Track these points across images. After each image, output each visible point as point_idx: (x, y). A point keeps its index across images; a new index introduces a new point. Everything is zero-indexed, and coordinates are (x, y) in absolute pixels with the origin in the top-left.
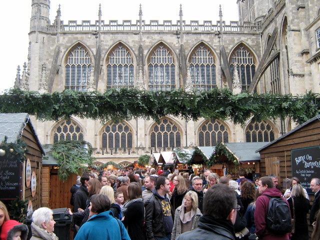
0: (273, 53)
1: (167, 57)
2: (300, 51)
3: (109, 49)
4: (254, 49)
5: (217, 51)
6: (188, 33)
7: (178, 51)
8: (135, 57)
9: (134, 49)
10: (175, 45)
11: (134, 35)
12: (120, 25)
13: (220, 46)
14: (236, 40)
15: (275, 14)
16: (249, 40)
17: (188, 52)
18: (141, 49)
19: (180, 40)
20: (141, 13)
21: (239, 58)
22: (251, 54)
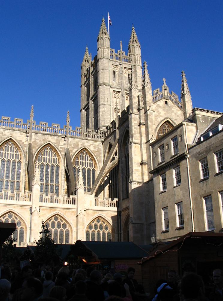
1: (15, 153)
2: (140, 161)
4: (95, 154)
5: (62, 153)
10: (23, 142)
14: (80, 145)
17: (35, 151)
19: (28, 138)
21: (82, 161)
22: (93, 159)
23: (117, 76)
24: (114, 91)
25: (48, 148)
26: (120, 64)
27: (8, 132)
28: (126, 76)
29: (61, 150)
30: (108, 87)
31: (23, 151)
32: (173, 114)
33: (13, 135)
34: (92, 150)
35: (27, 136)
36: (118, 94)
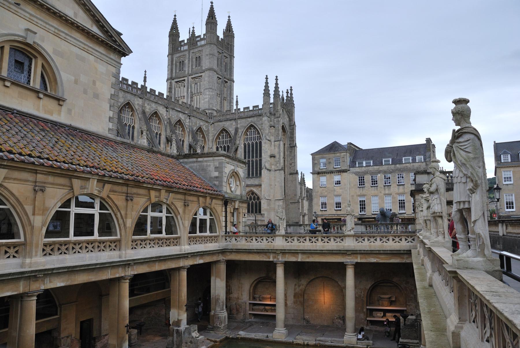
0: (236, 147)
2: (270, 154)
3: (121, 105)
6: (173, 109)
7: (166, 122)
8: (138, 120)
9: (138, 112)
10: (164, 117)
11: (139, 99)
12: (129, 85)
13: (189, 126)
15: (237, 117)
16: (204, 126)
18: (144, 112)
20: (145, 81)
22: (204, 137)
23: (219, 63)
24: (218, 77)
25: (178, 123)
26: (223, 52)
27: (155, 105)
28: (224, 63)
29: (187, 126)
30: (216, 73)
31: (164, 125)
32: (285, 120)
33: (158, 107)
34: (205, 129)
35: (167, 111)
36: (219, 80)
